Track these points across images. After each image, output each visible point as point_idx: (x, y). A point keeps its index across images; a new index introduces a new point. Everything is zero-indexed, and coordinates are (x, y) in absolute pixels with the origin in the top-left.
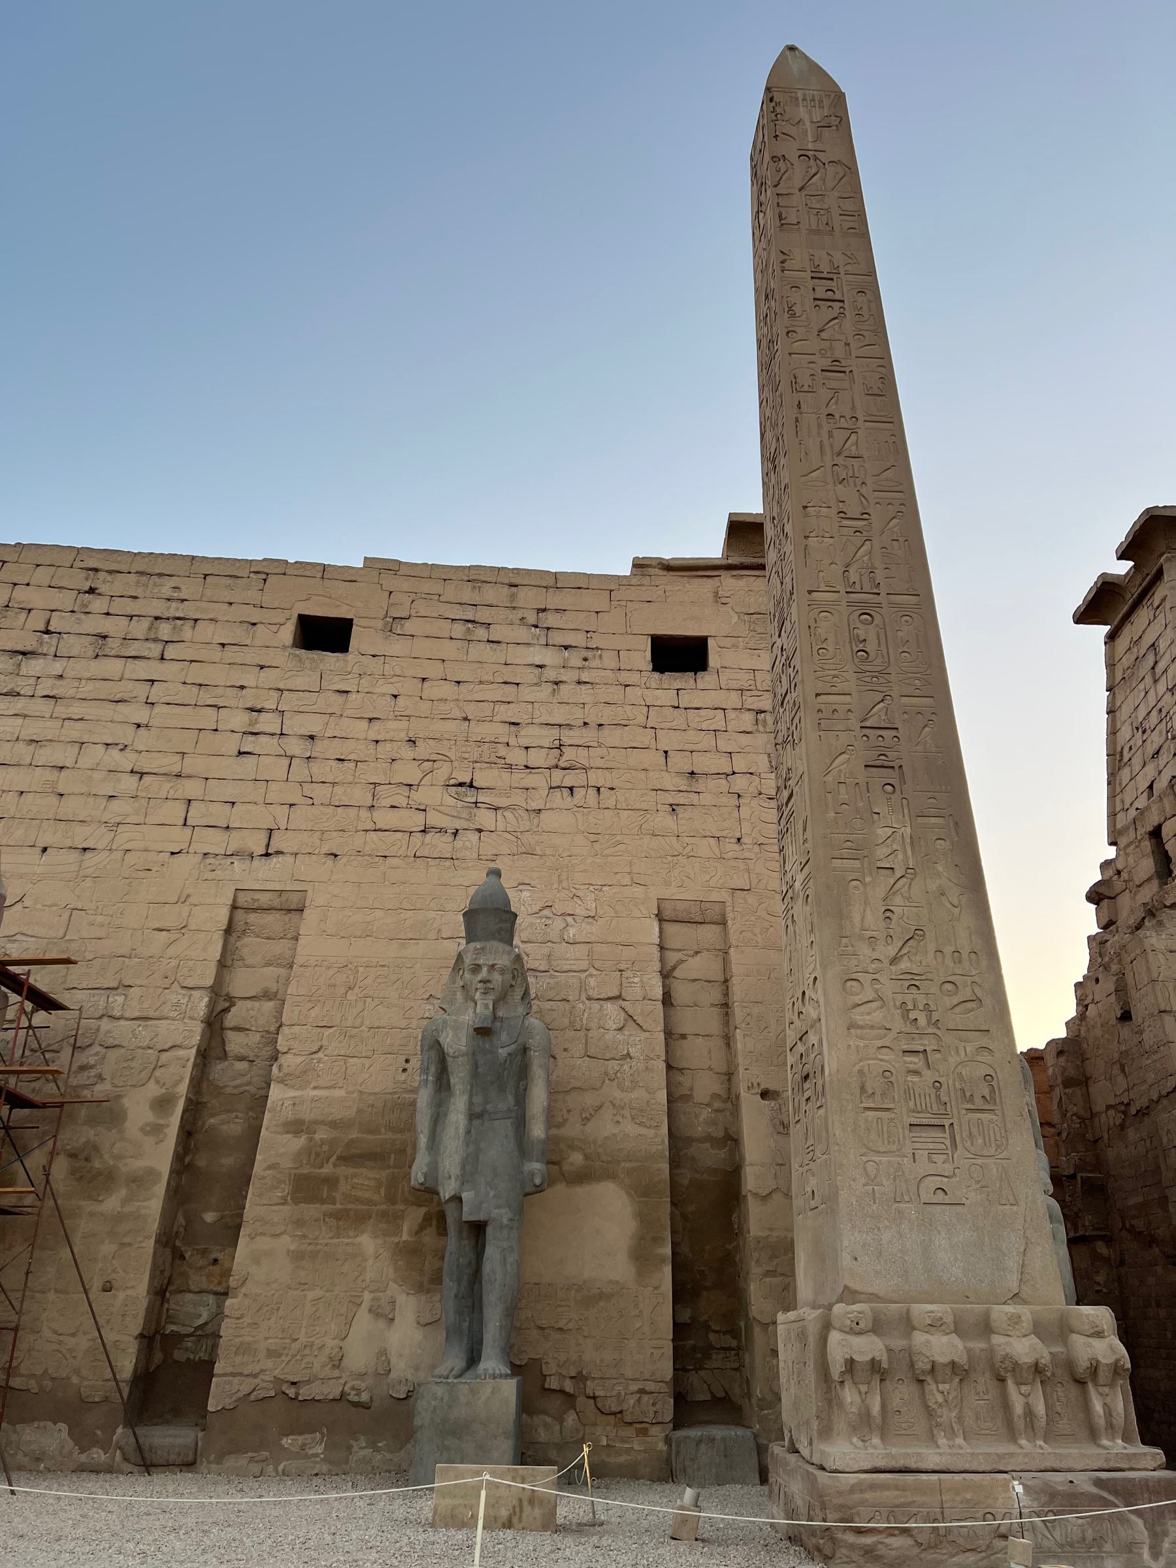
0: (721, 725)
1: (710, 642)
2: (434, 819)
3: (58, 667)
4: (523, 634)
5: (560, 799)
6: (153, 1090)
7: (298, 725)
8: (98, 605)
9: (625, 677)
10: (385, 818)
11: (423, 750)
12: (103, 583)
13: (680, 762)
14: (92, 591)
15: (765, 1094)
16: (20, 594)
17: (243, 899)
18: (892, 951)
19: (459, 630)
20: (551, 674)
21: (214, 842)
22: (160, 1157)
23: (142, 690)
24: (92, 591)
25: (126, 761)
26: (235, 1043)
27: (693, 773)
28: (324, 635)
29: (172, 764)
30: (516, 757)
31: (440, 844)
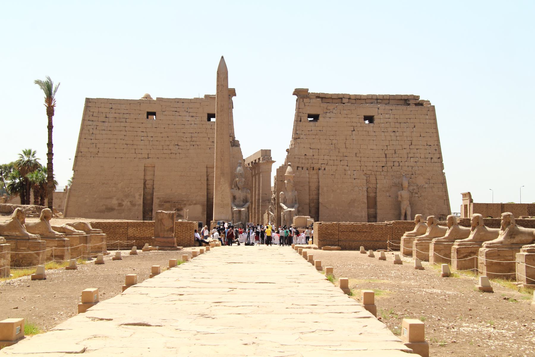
2: (172, 151)
3: (110, 124)
4: (185, 113)
5: (192, 147)
6: (138, 194)
7: (150, 134)
8: (113, 111)
9: (202, 122)
10: (165, 151)
16: (100, 109)
19: (174, 113)
20: (189, 122)
21: (140, 156)
22: (141, 202)
23: (124, 128)
25: (124, 142)
26: (147, 186)
29: (131, 142)
30: (185, 139)
31: (173, 156)
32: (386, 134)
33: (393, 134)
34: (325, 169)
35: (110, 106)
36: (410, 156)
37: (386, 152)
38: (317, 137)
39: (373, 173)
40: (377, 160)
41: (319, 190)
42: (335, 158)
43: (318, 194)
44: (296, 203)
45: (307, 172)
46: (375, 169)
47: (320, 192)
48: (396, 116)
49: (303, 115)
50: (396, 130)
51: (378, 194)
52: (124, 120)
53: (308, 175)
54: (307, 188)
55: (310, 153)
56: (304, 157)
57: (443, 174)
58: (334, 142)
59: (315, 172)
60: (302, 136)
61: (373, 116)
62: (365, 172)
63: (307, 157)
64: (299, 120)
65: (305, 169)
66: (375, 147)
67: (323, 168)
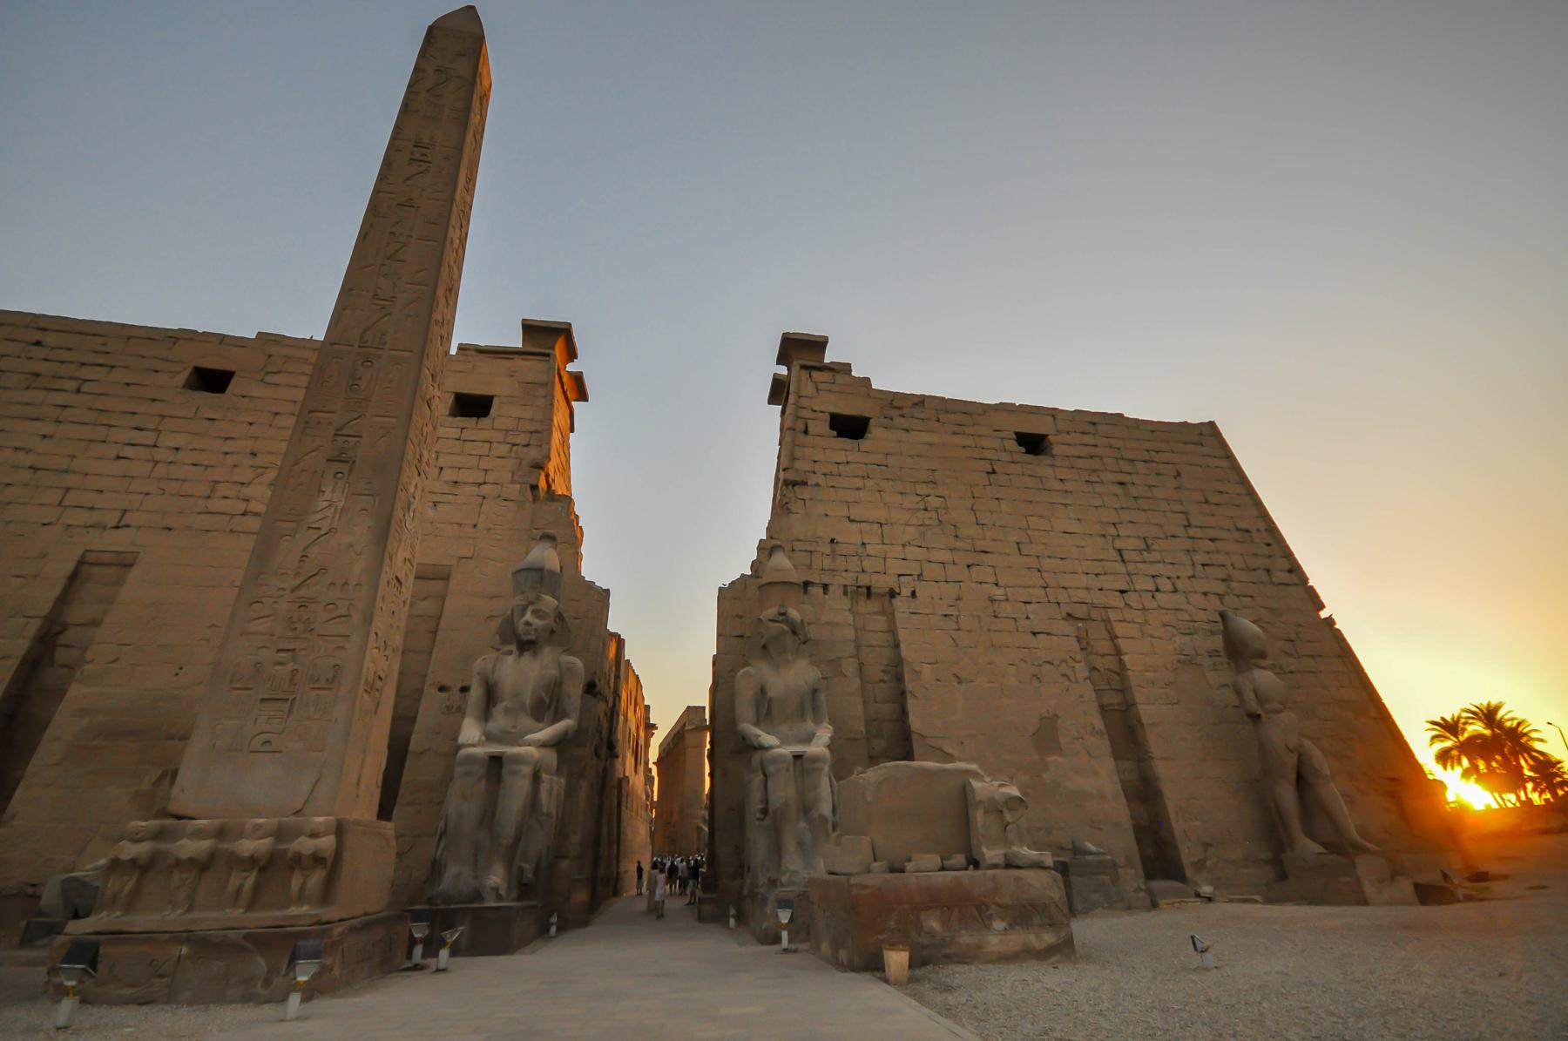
0: (485, 451)
1: (495, 401)
8: (38, 352)
10: (217, 504)
11: (260, 461)
12: (49, 339)
13: (449, 475)
14: (38, 343)
17: (90, 557)
18: (298, 582)
24: (38, 343)
28: (212, 381)
32: (1098, 488)
33: (1119, 490)
34: (913, 594)
35: (37, 336)
36: (1200, 558)
37: (1118, 544)
38: (870, 483)
39: (1095, 614)
40: (1098, 567)
41: (899, 678)
42: (946, 556)
43: (900, 696)
44: (817, 721)
45: (846, 603)
46: (1098, 598)
47: (910, 685)
48: (1118, 444)
49: (812, 415)
50: (1126, 478)
51: (1139, 695)
52: (73, 385)
53: (849, 617)
54: (850, 667)
55: (850, 536)
56: (827, 549)
57: (1330, 621)
58: (934, 502)
59: (874, 605)
60: (812, 480)
61: (1043, 437)
62: (1065, 609)
63: (839, 549)
64: (801, 427)
66: (1075, 528)
67: (906, 592)
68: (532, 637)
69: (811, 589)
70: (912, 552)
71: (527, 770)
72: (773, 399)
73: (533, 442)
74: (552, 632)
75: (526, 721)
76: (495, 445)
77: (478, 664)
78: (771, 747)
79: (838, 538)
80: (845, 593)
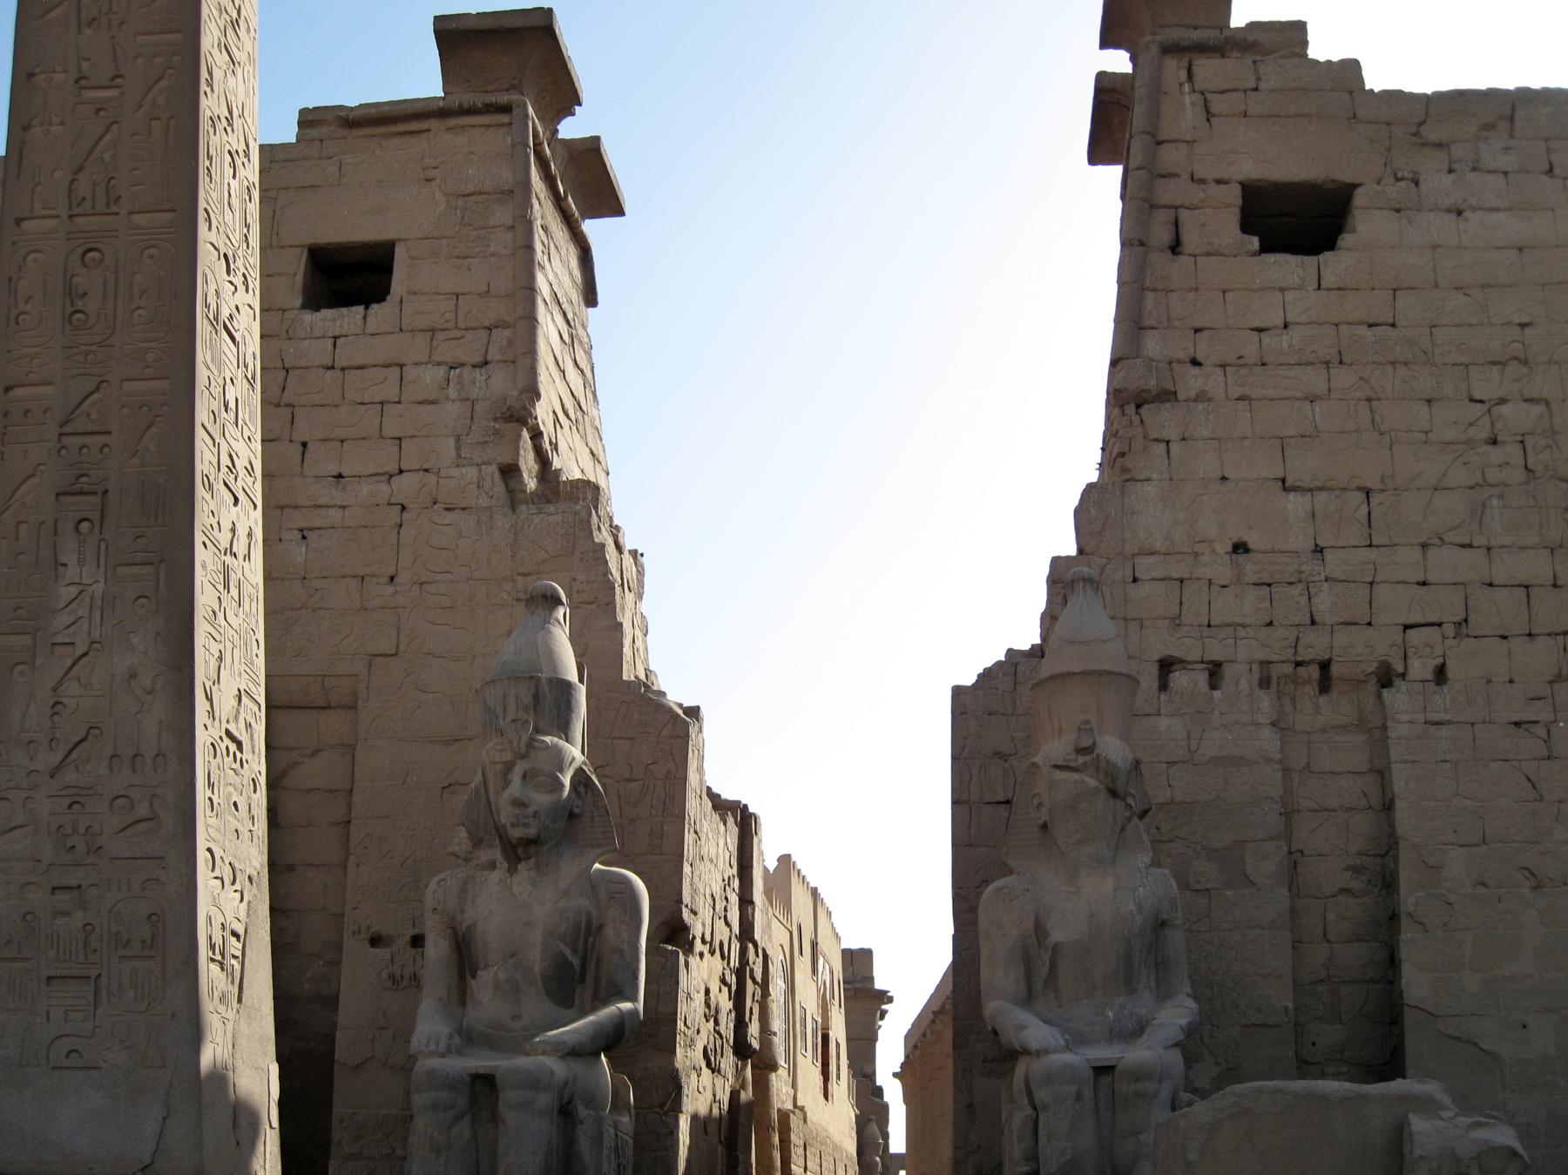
15: (375, 941)
27: (340, 476)
44: (1164, 993)
45: (1266, 701)
56: (1221, 571)
63: (1251, 568)
65: (1239, 677)
68: (532, 832)
69: (1179, 679)
70: (1448, 563)
71: (544, 1100)
72: (1099, 152)
73: (493, 354)
74: (572, 816)
75: (535, 1004)
76: (410, 373)
77: (433, 891)
78: (1046, 1051)
79: (1252, 541)
80: (1265, 682)
